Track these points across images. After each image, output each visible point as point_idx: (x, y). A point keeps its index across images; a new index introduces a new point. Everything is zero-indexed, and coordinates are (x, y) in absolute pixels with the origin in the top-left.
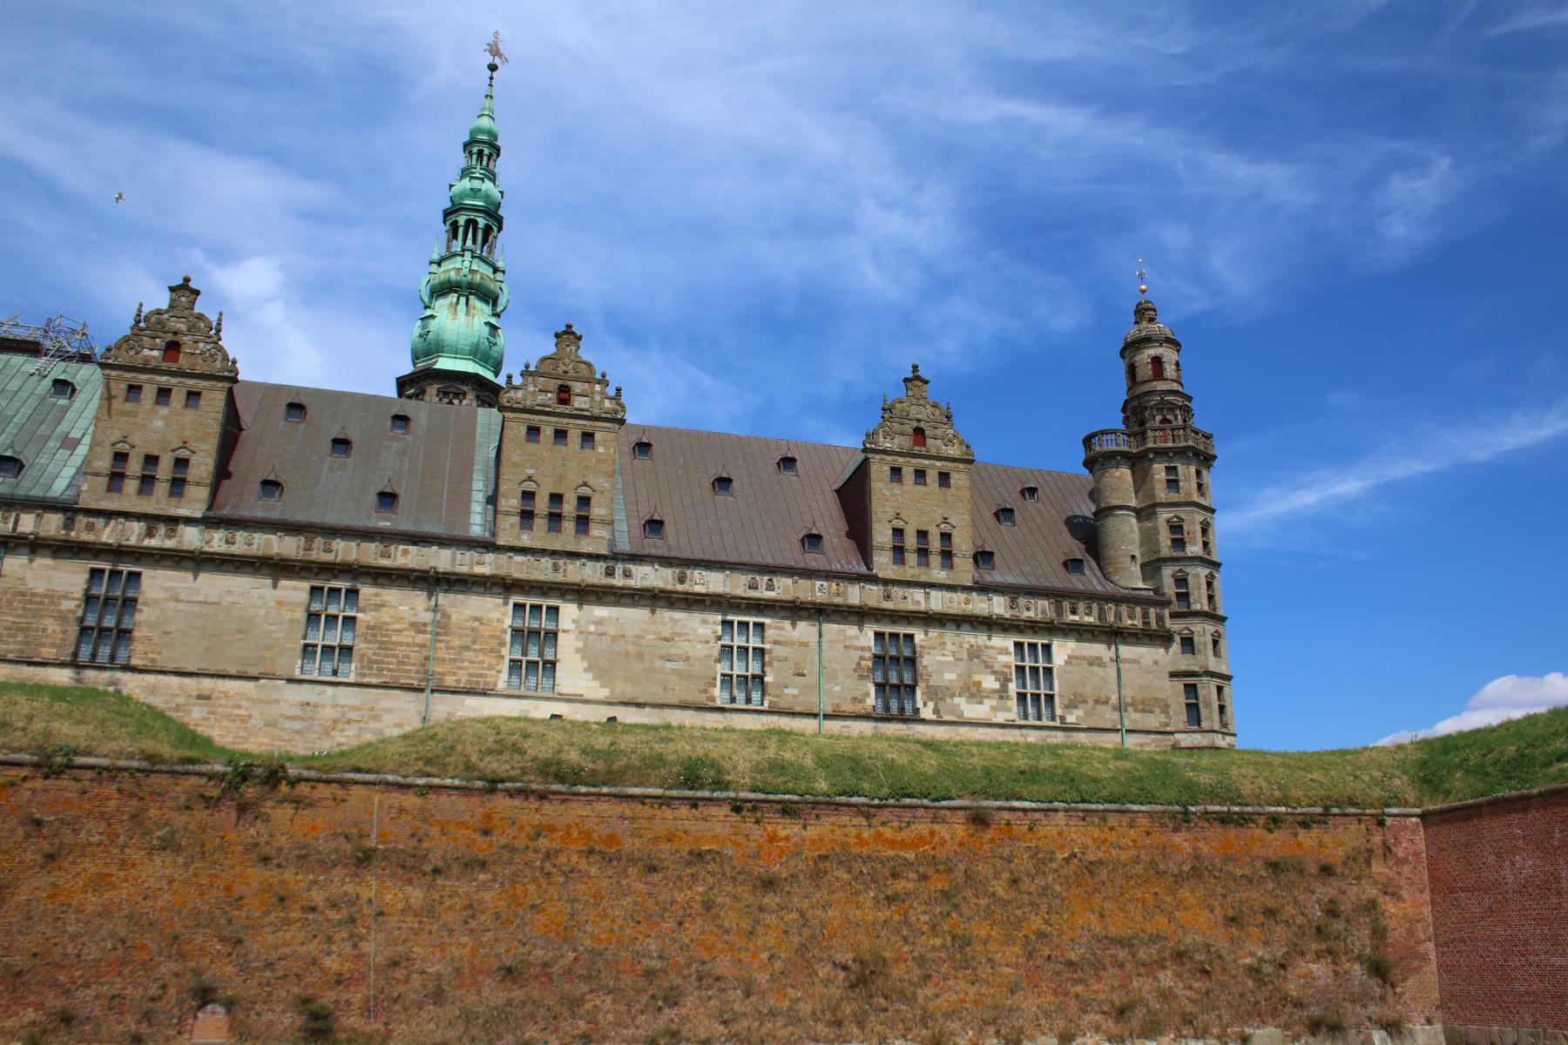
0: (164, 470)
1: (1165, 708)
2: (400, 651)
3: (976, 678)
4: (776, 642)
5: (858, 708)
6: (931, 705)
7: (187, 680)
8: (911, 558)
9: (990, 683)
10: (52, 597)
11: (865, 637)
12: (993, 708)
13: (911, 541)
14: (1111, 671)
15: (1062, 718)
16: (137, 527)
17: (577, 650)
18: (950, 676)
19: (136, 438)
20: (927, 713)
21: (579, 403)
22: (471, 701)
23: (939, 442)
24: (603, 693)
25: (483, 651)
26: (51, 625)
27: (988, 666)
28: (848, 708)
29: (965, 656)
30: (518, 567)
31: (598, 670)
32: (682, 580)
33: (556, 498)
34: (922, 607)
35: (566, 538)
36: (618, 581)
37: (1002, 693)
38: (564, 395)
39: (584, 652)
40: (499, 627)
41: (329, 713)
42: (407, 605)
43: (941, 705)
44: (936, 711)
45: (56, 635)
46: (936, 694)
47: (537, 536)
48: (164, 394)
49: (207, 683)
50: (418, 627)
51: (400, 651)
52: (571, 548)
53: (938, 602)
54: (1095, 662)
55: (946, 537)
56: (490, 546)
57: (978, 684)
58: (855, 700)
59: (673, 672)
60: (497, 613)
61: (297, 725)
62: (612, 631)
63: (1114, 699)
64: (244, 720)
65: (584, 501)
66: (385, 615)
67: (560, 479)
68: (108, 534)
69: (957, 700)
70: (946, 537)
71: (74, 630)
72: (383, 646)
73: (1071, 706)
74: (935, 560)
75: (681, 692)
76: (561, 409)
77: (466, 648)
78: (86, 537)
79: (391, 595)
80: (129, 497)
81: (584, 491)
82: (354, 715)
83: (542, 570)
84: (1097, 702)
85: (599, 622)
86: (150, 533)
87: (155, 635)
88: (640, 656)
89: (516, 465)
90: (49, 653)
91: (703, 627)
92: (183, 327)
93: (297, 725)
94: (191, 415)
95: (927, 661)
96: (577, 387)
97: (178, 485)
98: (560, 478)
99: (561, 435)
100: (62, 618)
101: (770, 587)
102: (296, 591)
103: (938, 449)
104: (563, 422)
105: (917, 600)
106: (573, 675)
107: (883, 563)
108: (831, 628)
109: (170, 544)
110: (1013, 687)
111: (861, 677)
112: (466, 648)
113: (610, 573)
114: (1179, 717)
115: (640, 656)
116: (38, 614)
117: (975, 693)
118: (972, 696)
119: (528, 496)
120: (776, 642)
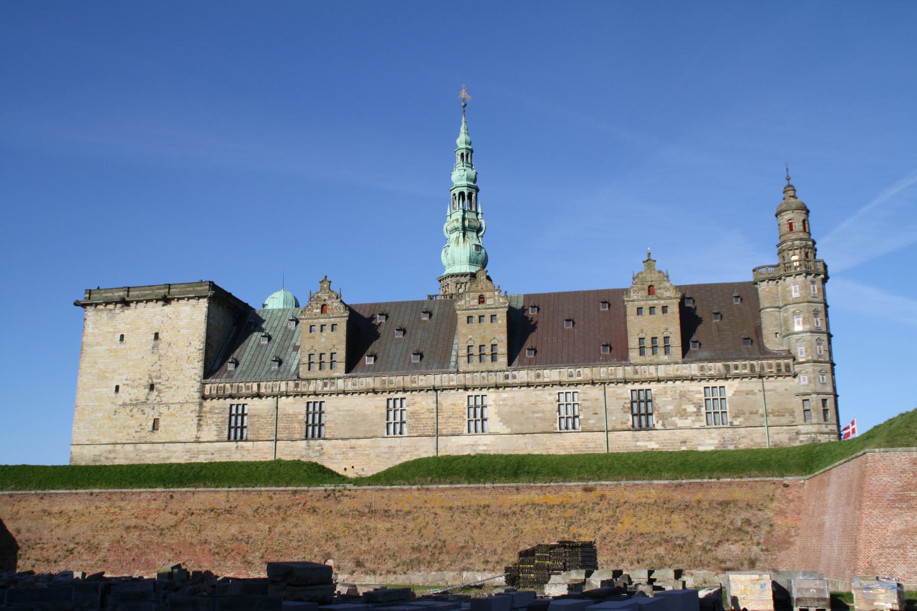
1: (792, 413)
2: (424, 421)
3: (684, 407)
4: (584, 400)
5: (624, 427)
6: (660, 422)
7: (346, 442)
8: (648, 351)
9: (691, 409)
10: (295, 415)
11: (626, 391)
12: (693, 421)
13: (648, 343)
14: (760, 396)
15: (731, 423)
16: (320, 383)
17: (496, 413)
18: (670, 408)
19: (316, 347)
20: (659, 426)
21: (489, 302)
22: (454, 439)
23: (662, 291)
24: (508, 431)
25: (457, 418)
26: (297, 425)
27: (690, 401)
28: (619, 427)
29: (678, 397)
30: (468, 379)
31: (505, 420)
32: (538, 376)
34: (654, 375)
35: (488, 364)
36: (510, 381)
38: (482, 300)
39: (499, 414)
40: (462, 407)
41: (399, 449)
42: (425, 402)
43: (666, 422)
44: (663, 425)
45: (299, 429)
46: (663, 417)
47: (475, 364)
49: (353, 442)
51: (424, 421)
52: (490, 368)
53: (662, 371)
54: (750, 392)
55: (666, 339)
57: (685, 410)
58: (622, 423)
59: (537, 418)
61: (387, 456)
62: (510, 403)
63: (762, 411)
64: (368, 455)
66: (416, 407)
67: (483, 338)
68: (312, 388)
69: (674, 419)
70: (666, 339)
71: (304, 426)
72: (418, 420)
73: (736, 416)
74: (661, 351)
75: (541, 426)
76: (481, 306)
77: (450, 417)
78: (304, 390)
79: (418, 397)
80: (316, 371)
81: (494, 342)
82: (408, 449)
83: (478, 379)
84: (751, 413)
85: (504, 400)
86: (325, 385)
87: (332, 425)
88: (523, 413)
89: (464, 335)
90: (297, 436)
91: (549, 396)
92: (327, 298)
93: (387, 456)
94: (334, 334)
95: (658, 401)
96: (487, 295)
98: (483, 338)
100: (299, 422)
101: (579, 375)
102: (381, 400)
103: (662, 294)
104: (481, 312)
105: (651, 371)
106: (494, 424)
107: (634, 355)
108: (611, 388)
109: (333, 388)
110: (703, 409)
111: (625, 412)
112: (450, 417)
113: (507, 377)
114: (799, 417)
115: (523, 413)
116: (291, 422)
117: (683, 414)
118: (682, 416)
120: (584, 400)
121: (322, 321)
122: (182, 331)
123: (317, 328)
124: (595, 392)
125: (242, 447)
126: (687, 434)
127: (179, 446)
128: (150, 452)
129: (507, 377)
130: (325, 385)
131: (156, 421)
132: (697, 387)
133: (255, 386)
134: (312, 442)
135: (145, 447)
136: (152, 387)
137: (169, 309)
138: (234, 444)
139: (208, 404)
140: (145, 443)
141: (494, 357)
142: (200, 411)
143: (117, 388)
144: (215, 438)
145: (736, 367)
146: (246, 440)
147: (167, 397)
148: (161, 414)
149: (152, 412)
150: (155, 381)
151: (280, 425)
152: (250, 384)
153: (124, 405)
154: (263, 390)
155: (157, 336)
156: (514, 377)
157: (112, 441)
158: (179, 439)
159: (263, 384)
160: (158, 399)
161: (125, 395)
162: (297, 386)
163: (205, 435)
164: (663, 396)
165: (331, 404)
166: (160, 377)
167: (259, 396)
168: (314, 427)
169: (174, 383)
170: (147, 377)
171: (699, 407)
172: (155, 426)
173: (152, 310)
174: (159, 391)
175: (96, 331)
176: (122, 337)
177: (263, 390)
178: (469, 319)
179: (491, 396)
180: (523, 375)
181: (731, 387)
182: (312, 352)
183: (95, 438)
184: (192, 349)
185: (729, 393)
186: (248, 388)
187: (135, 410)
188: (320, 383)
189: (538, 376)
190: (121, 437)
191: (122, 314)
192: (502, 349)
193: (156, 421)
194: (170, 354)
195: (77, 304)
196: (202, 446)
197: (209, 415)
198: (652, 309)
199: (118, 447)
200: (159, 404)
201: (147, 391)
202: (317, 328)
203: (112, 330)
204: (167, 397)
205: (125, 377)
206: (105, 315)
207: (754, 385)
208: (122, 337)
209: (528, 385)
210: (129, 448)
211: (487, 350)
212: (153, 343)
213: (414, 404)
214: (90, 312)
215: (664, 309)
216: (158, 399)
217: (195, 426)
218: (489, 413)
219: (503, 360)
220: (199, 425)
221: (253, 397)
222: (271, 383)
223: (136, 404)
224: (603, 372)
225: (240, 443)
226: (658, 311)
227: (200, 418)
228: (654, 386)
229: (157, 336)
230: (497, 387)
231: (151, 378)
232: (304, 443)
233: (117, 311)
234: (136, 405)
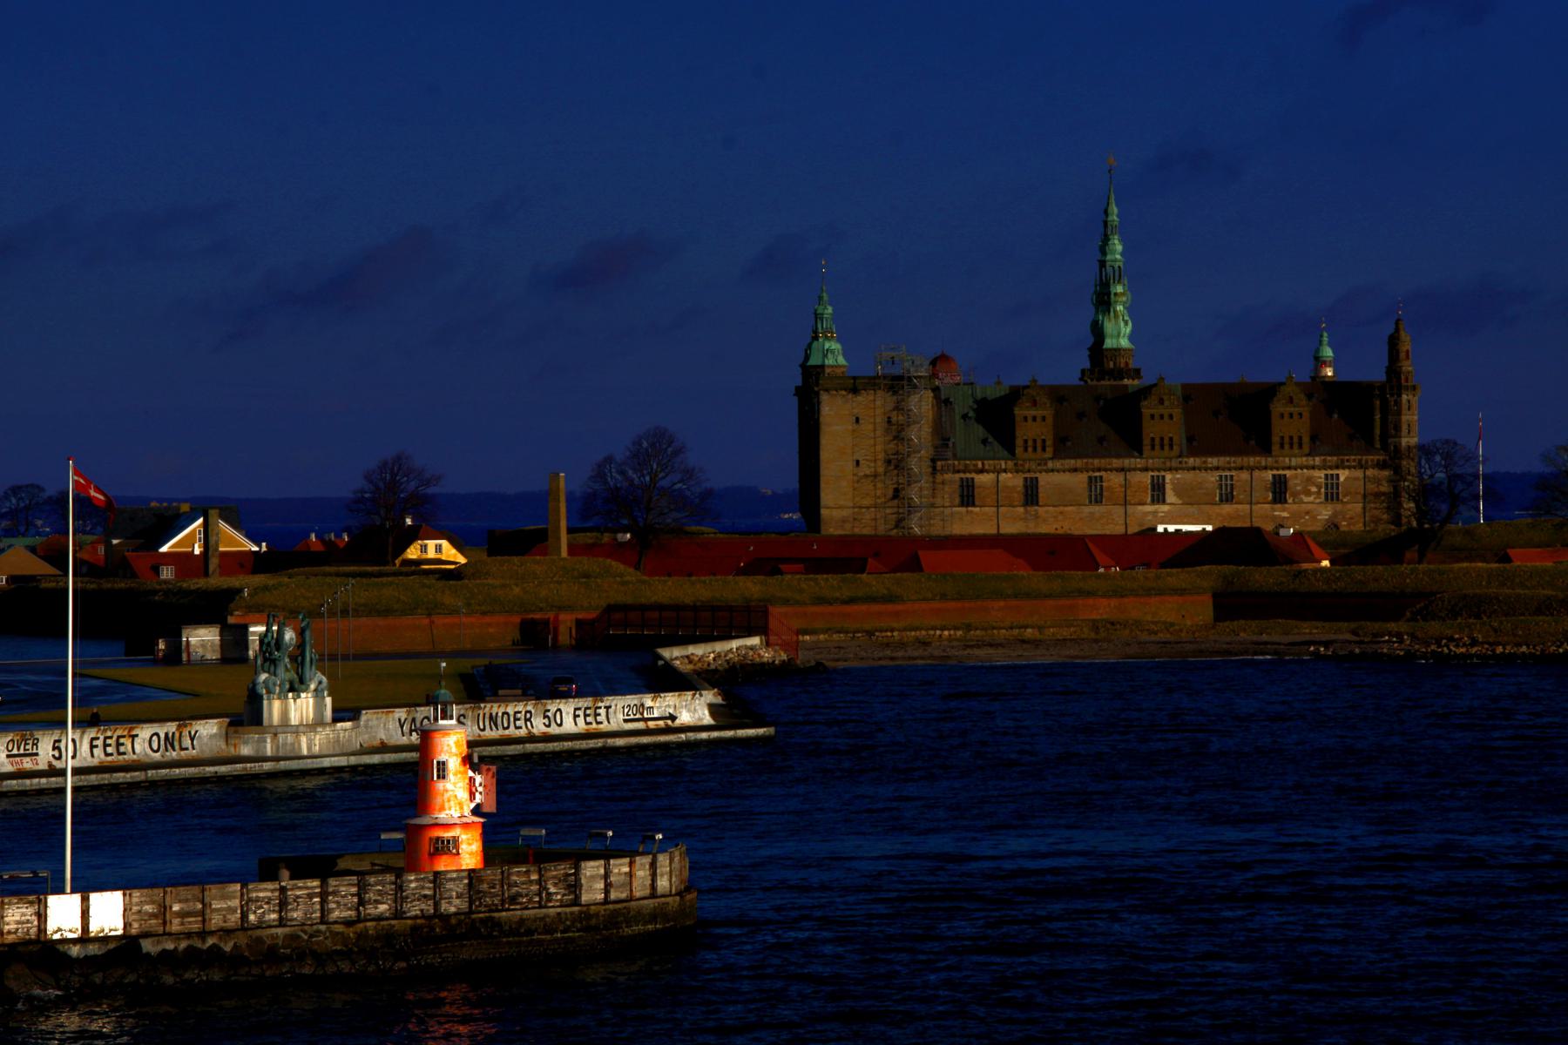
9: (1314, 489)
31: (1178, 493)
37: (1319, 493)
45: (1018, 497)
48: (1034, 419)
53: (1294, 462)
54: (1357, 479)
60: (1146, 478)
91: (1213, 477)
95: (1291, 483)
99: (1162, 417)
106: (1171, 497)
108: (1256, 473)
117: (1308, 493)
124: (1245, 475)
126: (1310, 507)
132: (1322, 474)
139: (939, 478)
153: (866, 476)
161: (865, 469)
163: (938, 501)
164: (1295, 478)
165: (1044, 480)
168: (1031, 495)
171: (1319, 487)
178: (1152, 417)
179: (1168, 477)
181: (1343, 475)
185: (1342, 479)
198: (1291, 415)
207: (1359, 473)
218: (1168, 487)
224: (1252, 460)
228: (1288, 473)
232: (1021, 509)
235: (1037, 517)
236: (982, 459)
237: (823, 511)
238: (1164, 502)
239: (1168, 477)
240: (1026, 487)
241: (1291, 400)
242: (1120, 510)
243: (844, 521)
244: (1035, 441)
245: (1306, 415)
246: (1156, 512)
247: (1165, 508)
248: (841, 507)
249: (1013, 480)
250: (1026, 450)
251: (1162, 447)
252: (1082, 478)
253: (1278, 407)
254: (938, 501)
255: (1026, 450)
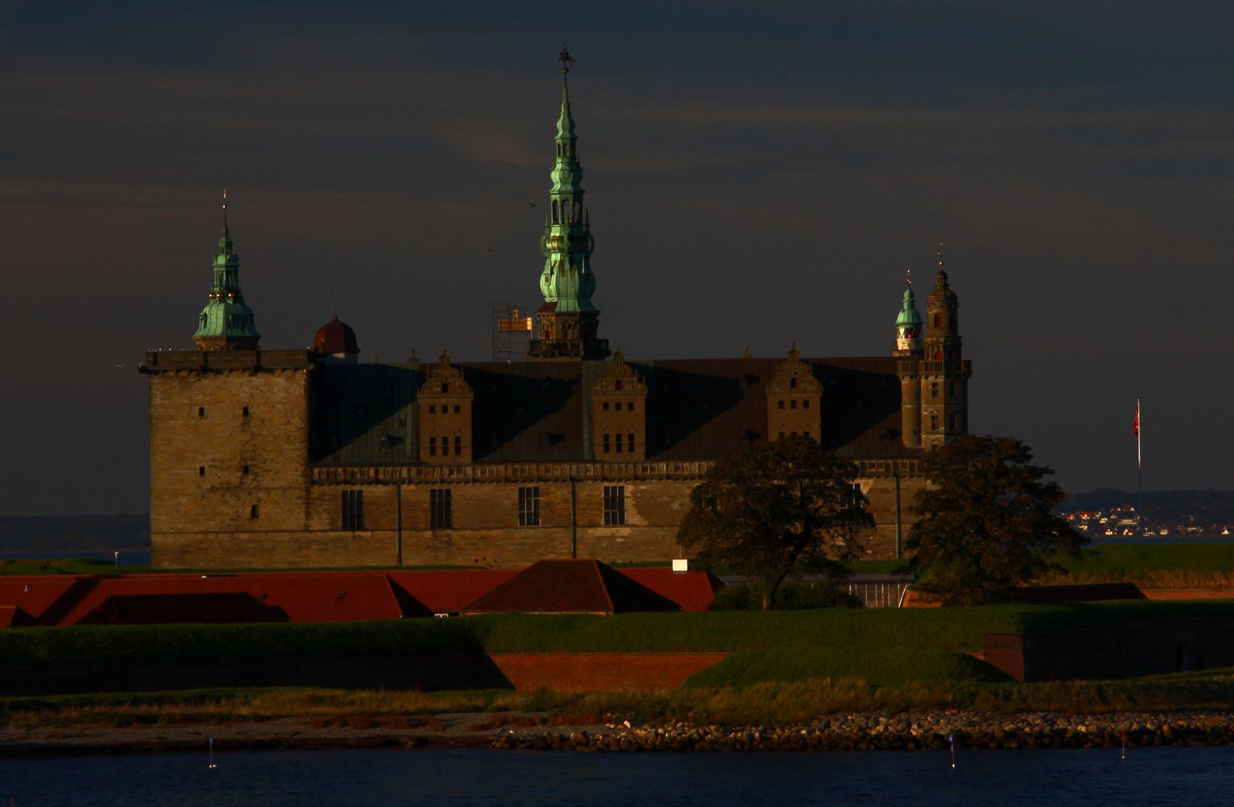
0: (451, 445)
21: (627, 387)
22: (590, 531)
24: (646, 523)
26: (419, 514)
31: (642, 512)
33: (619, 437)
39: (636, 506)
48: (445, 409)
49: (484, 532)
50: (566, 501)
54: (885, 491)
56: (594, 461)
65: (631, 437)
79: (552, 487)
84: (884, 511)
85: (643, 491)
90: (422, 526)
97: (458, 451)
106: (632, 516)
113: (645, 469)
119: (606, 437)
121: (444, 401)
122: (277, 406)
123: (439, 410)
125: (360, 537)
127: (286, 536)
128: (250, 541)
129: (645, 469)
130: (451, 472)
131: (254, 510)
133: (372, 472)
134: (438, 532)
135: (244, 536)
136: (246, 470)
137: (258, 380)
138: (349, 534)
139: (316, 490)
140: (244, 532)
141: (632, 448)
142: (308, 497)
143: (202, 470)
144: (327, 527)
145: (873, 466)
146: (365, 530)
147: (266, 481)
148: (259, 500)
149: (248, 498)
150: (249, 462)
151: (403, 514)
152: (365, 469)
153: (213, 489)
154: (381, 476)
155: (246, 411)
156: (653, 469)
157: (203, 529)
158: (284, 527)
159: (381, 469)
160: (255, 483)
161: (212, 479)
162: (419, 472)
163: (315, 524)
165: (459, 493)
166: (255, 459)
167: (378, 482)
168: (441, 514)
169: (272, 466)
170: (238, 458)
172: (254, 513)
173: (237, 380)
174: (256, 475)
175: (166, 402)
176: (202, 411)
177: (381, 476)
178: (606, 406)
180: (663, 467)
182: (434, 435)
183: (181, 526)
184: (291, 428)
186: (362, 473)
187: (228, 495)
188: (446, 470)
189: (676, 469)
190: (213, 525)
191: (198, 384)
192: (640, 439)
193: (254, 510)
194: (265, 432)
195: (143, 370)
196: (312, 536)
197: (318, 502)
199: (211, 536)
200: (258, 488)
201: (239, 474)
202: (439, 410)
203: (186, 401)
204: (266, 481)
205: (210, 457)
206: (175, 383)
207: (889, 484)
208: (202, 411)
209: (668, 477)
210: (223, 537)
211: (625, 440)
212: (241, 419)
213: (549, 494)
214: (156, 380)
215: (806, 404)
216: (255, 483)
217: (302, 514)
218: (629, 503)
219: (640, 450)
220: (308, 515)
221: (370, 483)
222: (390, 469)
223: (226, 488)
225: (357, 533)
226: (800, 405)
227: (308, 505)
229: (246, 411)
230: (636, 478)
231: (243, 459)
232: (428, 534)
233: (192, 379)
234: (228, 490)
235: (450, 543)
236: (376, 465)
237: (156, 539)
238: (622, 522)
239: (629, 489)
240: (433, 503)
241: (794, 383)
242: (563, 535)
243: (184, 550)
244: (445, 440)
245: (816, 404)
246: (613, 537)
247: (624, 531)
248: (180, 532)
249: (508, 495)
250: (433, 452)
251: (619, 449)
252: (513, 491)
253: (777, 391)
254: (315, 524)
255: (433, 452)
